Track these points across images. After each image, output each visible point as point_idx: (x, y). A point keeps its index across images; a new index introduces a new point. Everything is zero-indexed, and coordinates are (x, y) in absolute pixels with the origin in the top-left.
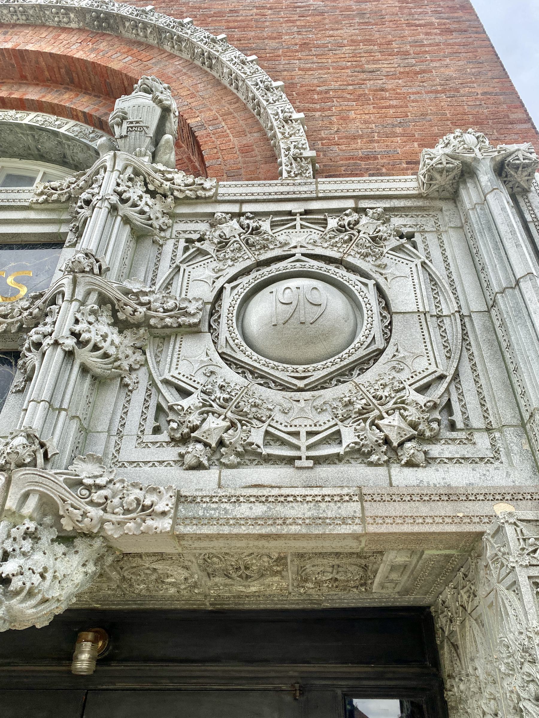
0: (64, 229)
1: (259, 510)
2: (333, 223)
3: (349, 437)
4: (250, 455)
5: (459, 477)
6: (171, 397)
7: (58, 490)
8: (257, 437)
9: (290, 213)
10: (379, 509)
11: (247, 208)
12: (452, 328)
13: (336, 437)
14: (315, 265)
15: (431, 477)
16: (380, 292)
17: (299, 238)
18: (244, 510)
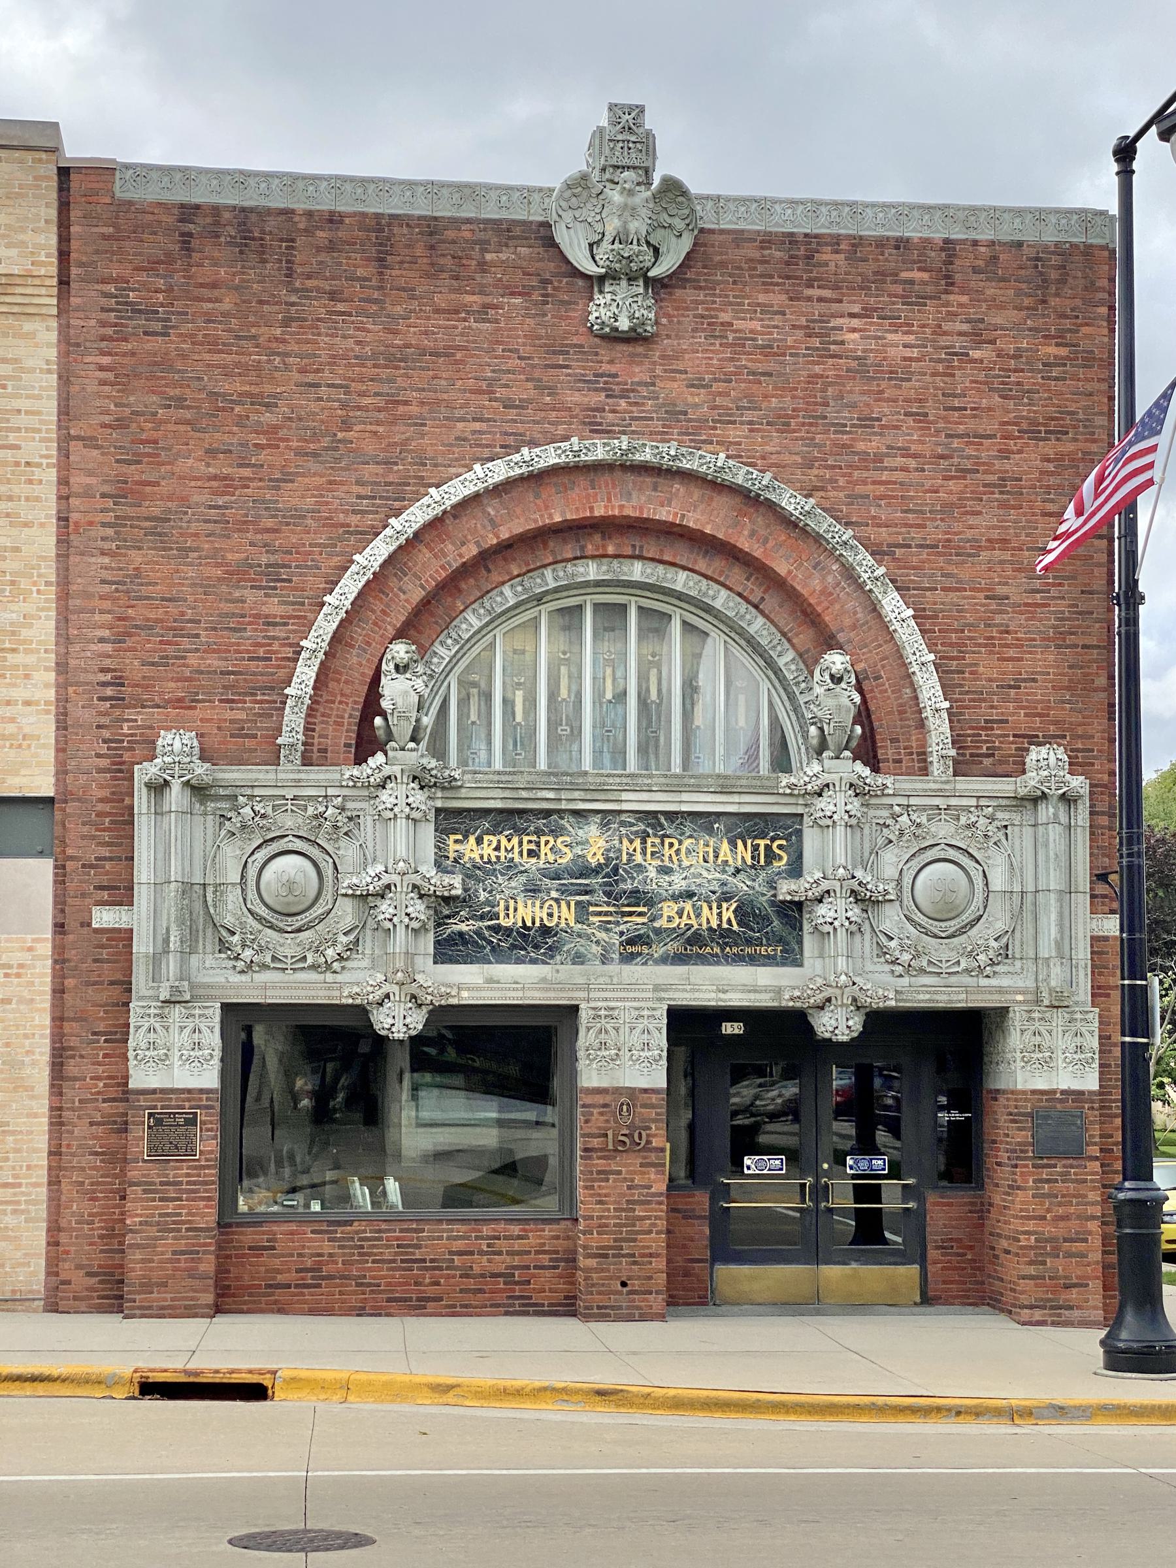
0: (800, 810)
1: (927, 996)
2: (963, 820)
3: (963, 965)
4: (922, 971)
5: (1005, 982)
6: (883, 939)
7: (858, 994)
8: (925, 964)
10: (973, 997)
11: (913, 801)
12: (1016, 898)
13: (958, 963)
14: (952, 854)
15: (993, 982)
16: (985, 876)
17: (943, 830)
18: (921, 997)
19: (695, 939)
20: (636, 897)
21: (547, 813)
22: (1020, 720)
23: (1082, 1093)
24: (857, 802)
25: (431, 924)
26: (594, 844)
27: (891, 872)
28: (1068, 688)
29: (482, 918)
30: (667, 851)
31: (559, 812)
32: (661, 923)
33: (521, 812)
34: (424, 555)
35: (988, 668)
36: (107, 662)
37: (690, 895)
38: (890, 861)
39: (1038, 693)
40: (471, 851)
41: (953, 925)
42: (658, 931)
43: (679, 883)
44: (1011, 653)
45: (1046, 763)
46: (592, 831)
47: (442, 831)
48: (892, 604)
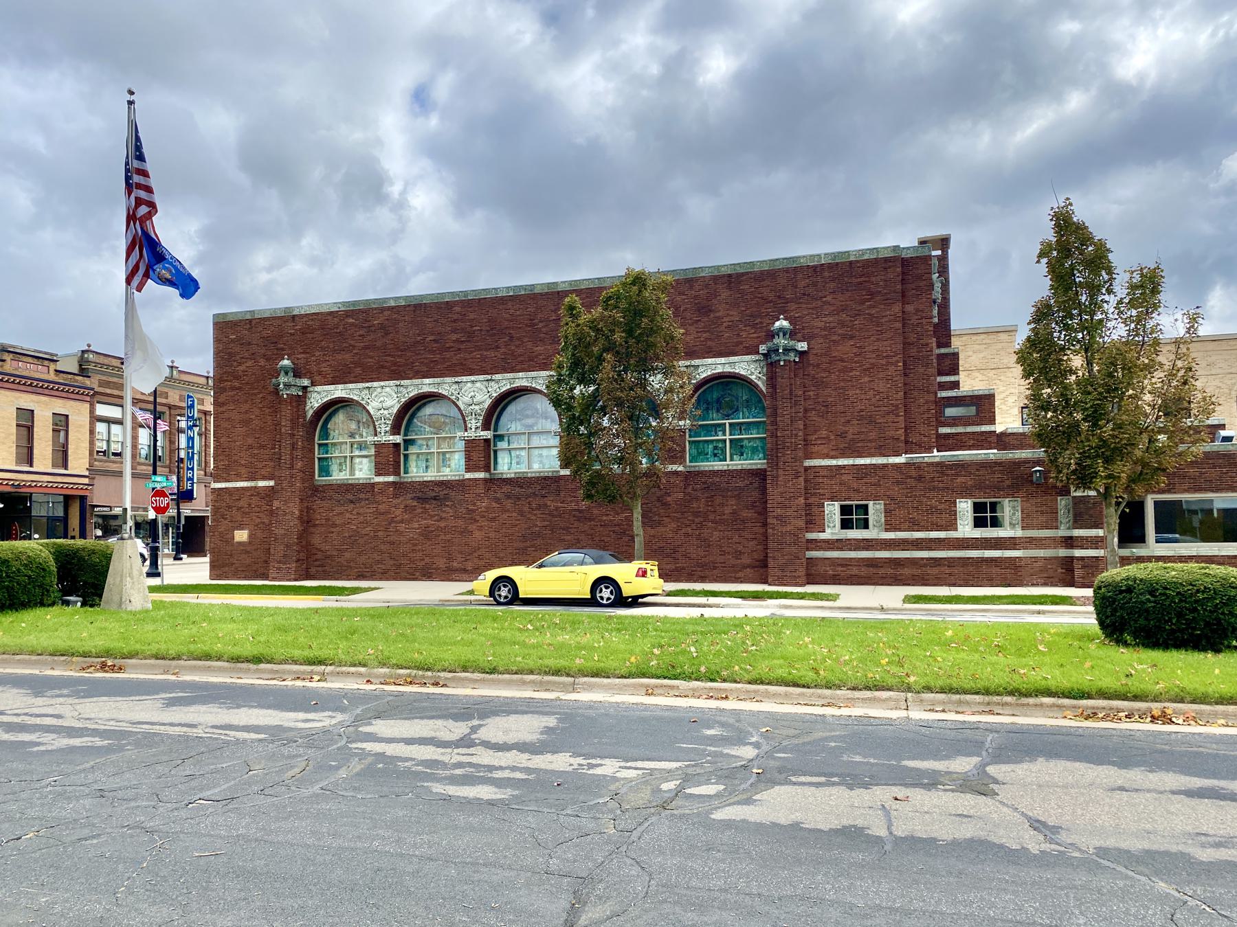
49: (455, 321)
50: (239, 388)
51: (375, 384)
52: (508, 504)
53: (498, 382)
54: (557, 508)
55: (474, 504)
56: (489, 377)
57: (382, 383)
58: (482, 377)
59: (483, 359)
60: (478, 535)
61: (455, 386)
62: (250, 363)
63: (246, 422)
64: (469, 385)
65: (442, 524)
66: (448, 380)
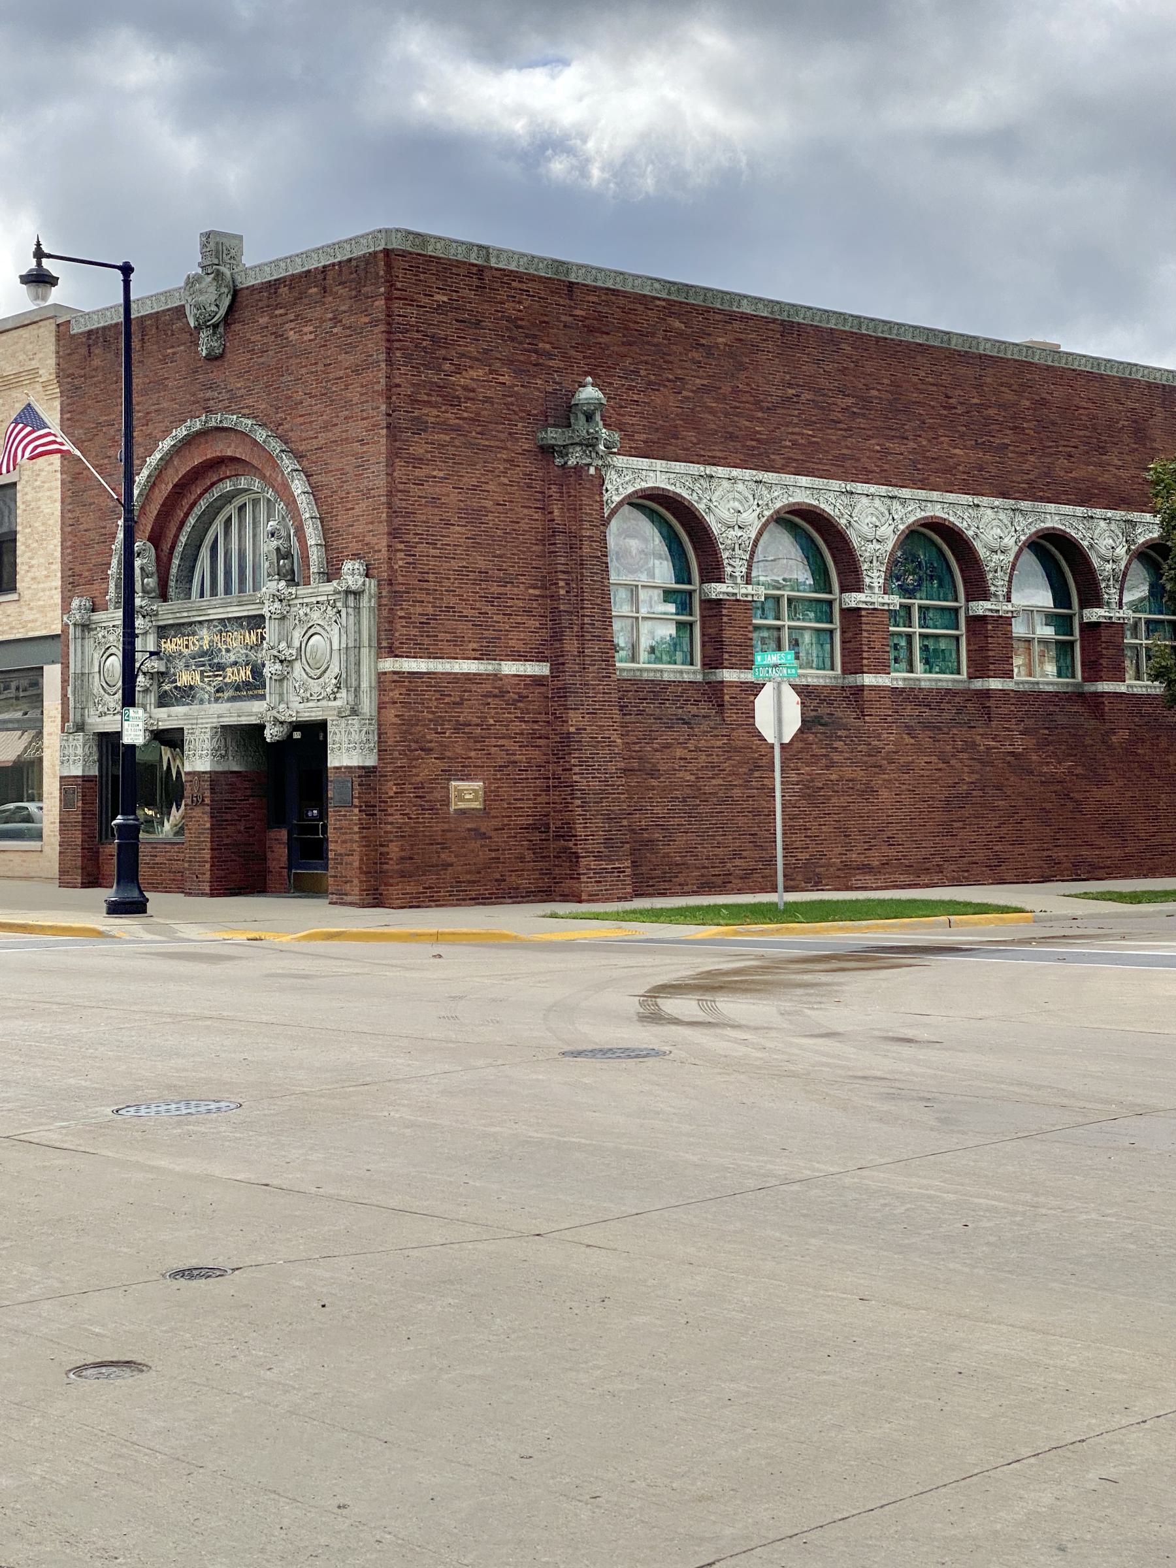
7: (278, 715)
9: (312, 603)
11: (306, 600)
14: (318, 629)
17: (315, 616)
19: (238, 689)
20: (221, 667)
21: (190, 624)
22: (354, 546)
23: (351, 767)
24: (277, 605)
25: (155, 687)
26: (205, 638)
27: (296, 644)
28: (372, 523)
29: (172, 682)
30: (229, 640)
31: (195, 622)
32: (227, 680)
33: (183, 624)
34: (157, 491)
35: (343, 519)
36: (70, 566)
37: (235, 663)
38: (297, 635)
39: (359, 528)
40: (169, 646)
41: (319, 672)
42: (226, 684)
43: (233, 659)
44: (350, 506)
45: (352, 574)
46: (204, 632)
47: (160, 637)
48: (298, 486)
49: (844, 371)
50: (456, 429)
51: (720, 471)
52: (924, 737)
53: (904, 501)
54: (989, 748)
55: (878, 737)
56: (895, 491)
57: (736, 472)
58: (883, 490)
59: (885, 452)
60: (884, 794)
61: (845, 499)
62: (478, 373)
63: (474, 516)
64: (864, 500)
65: (833, 777)
66: (836, 484)
